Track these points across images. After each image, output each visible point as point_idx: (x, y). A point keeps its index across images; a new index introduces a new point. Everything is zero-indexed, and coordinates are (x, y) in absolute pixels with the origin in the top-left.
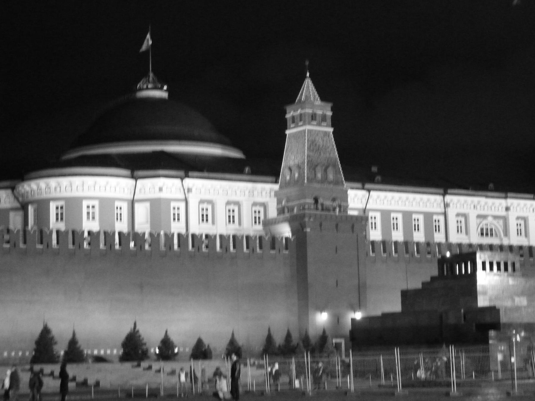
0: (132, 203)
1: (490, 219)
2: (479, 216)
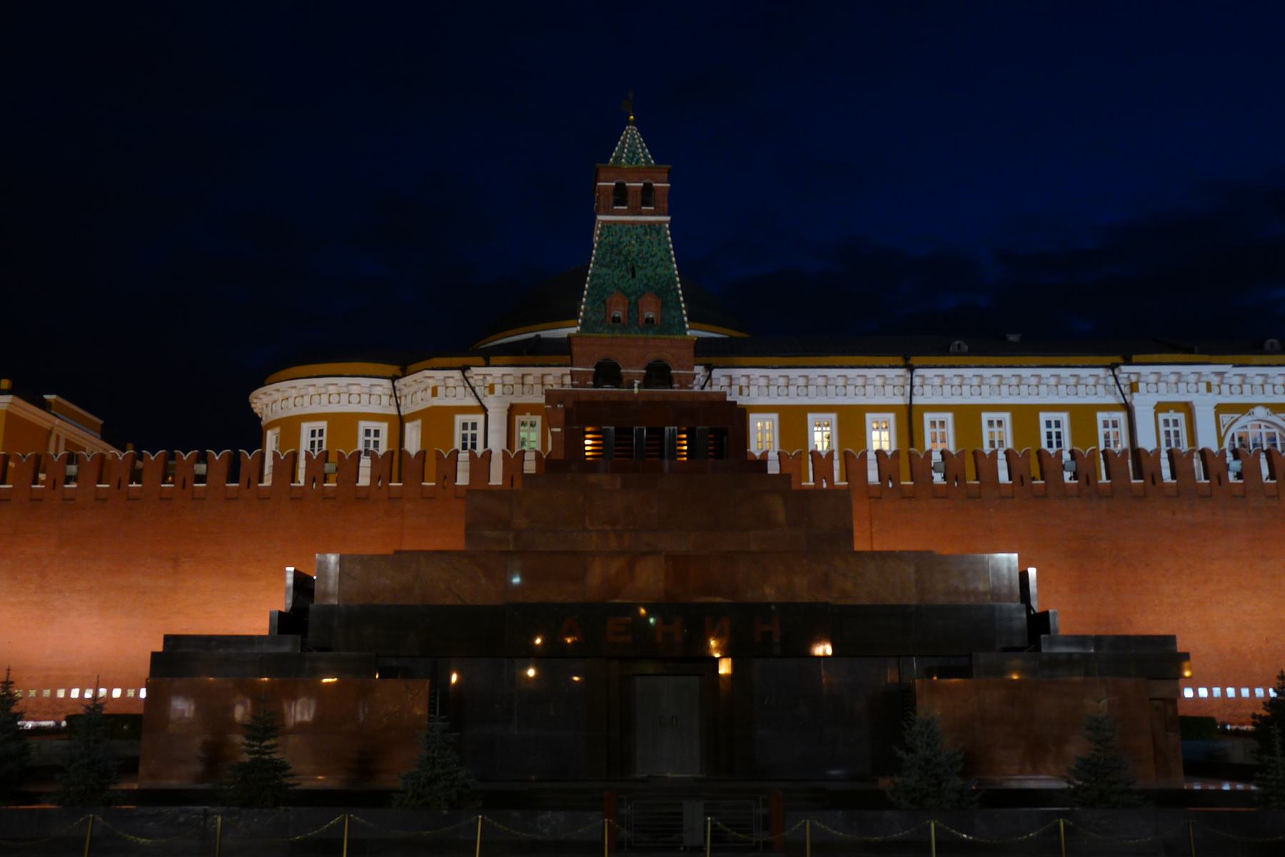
0: (399, 423)
1: (1260, 412)
2: (1220, 409)
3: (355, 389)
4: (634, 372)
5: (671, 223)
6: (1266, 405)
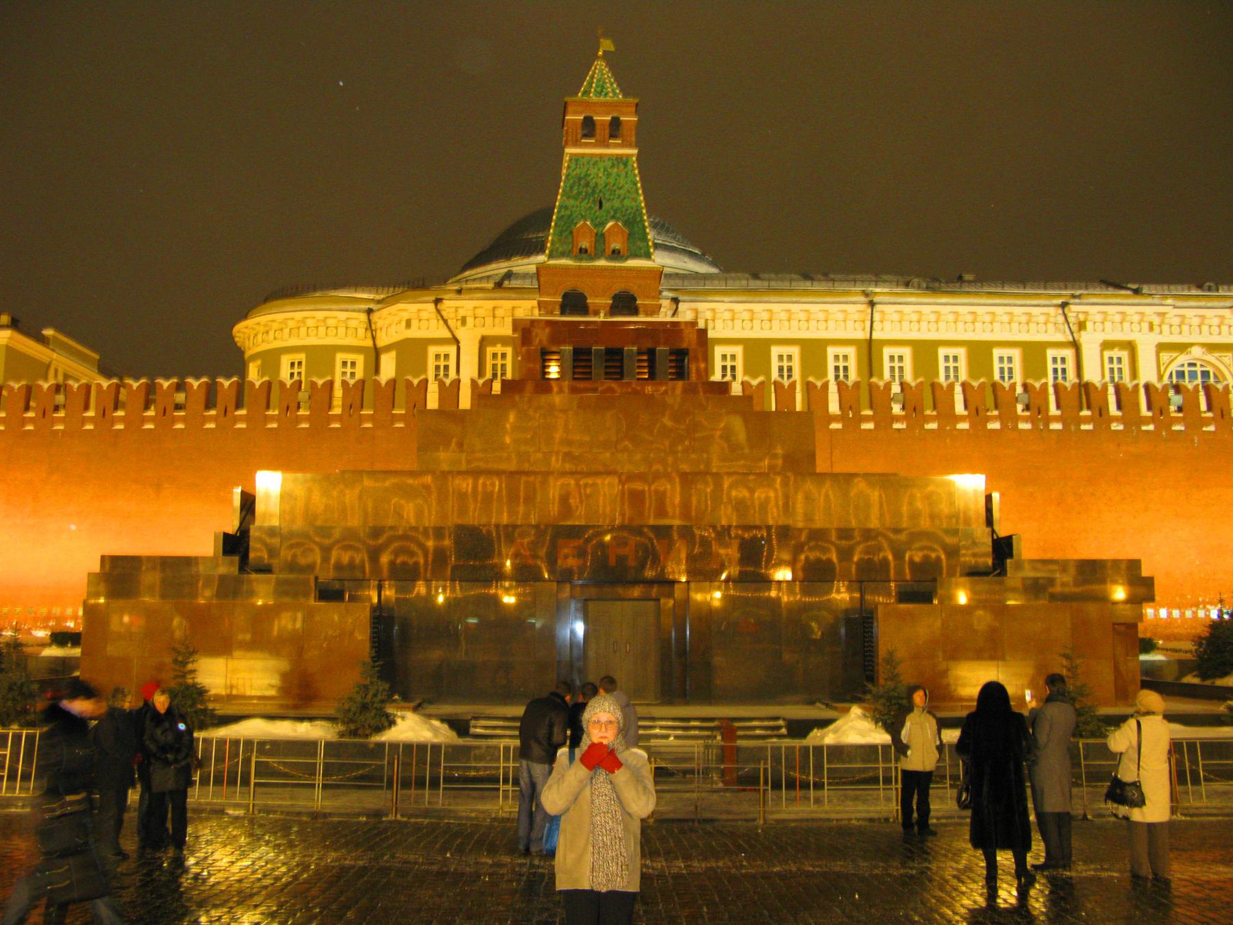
1: (1196, 352)
2: (1161, 347)
3: (331, 322)
4: (600, 300)
5: (639, 156)
6: (1203, 345)
